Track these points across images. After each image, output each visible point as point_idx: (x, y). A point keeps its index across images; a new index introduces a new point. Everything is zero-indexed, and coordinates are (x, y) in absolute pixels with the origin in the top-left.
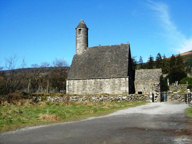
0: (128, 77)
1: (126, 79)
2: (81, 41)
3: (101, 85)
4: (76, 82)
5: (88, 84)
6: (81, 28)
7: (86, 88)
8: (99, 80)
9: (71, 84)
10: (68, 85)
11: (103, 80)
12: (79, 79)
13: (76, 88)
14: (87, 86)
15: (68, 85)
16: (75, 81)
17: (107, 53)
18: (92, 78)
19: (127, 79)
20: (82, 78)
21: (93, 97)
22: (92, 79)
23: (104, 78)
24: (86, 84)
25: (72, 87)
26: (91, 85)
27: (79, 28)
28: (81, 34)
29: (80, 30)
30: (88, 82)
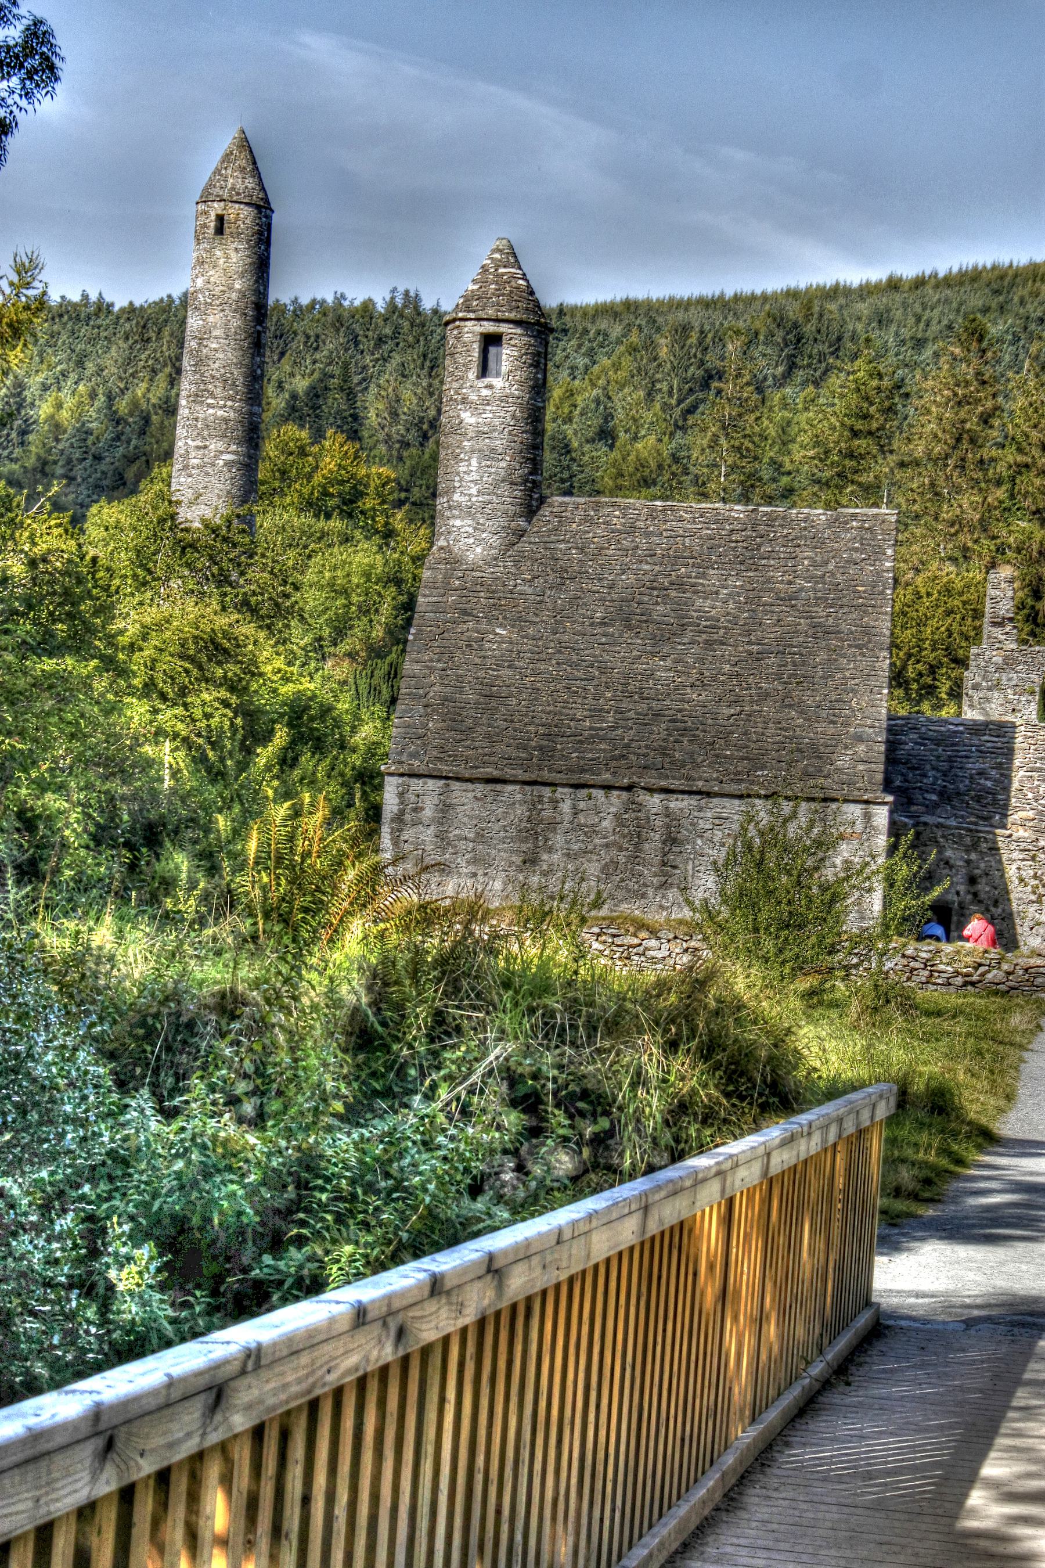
0: (890, 798)
1: (868, 817)
2: (500, 443)
3: (671, 840)
4: (463, 795)
5: (566, 825)
6: (504, 328)
7: (550, 850)
8: (654, 803)
9: (428, 813)
10: (402, 813)
11: (692, 801)
12: (496, 773)
13: (462, 845)
14: (558, 839)
15: (399, 818)
16: (456, 785)
17: (714, 577)
18: (606, 777)
19: (881, 816)
20: (520, 774)
21: (653, 943)
22: (607, 788)
23: (699, 793)
24: (553, 825)
25: (428, 835)
26: (593, 831)
27: (490, 327)
28: (498, 383)
29: (491, 340)
30: (566, 807)
